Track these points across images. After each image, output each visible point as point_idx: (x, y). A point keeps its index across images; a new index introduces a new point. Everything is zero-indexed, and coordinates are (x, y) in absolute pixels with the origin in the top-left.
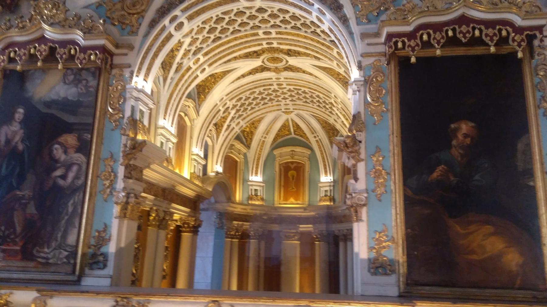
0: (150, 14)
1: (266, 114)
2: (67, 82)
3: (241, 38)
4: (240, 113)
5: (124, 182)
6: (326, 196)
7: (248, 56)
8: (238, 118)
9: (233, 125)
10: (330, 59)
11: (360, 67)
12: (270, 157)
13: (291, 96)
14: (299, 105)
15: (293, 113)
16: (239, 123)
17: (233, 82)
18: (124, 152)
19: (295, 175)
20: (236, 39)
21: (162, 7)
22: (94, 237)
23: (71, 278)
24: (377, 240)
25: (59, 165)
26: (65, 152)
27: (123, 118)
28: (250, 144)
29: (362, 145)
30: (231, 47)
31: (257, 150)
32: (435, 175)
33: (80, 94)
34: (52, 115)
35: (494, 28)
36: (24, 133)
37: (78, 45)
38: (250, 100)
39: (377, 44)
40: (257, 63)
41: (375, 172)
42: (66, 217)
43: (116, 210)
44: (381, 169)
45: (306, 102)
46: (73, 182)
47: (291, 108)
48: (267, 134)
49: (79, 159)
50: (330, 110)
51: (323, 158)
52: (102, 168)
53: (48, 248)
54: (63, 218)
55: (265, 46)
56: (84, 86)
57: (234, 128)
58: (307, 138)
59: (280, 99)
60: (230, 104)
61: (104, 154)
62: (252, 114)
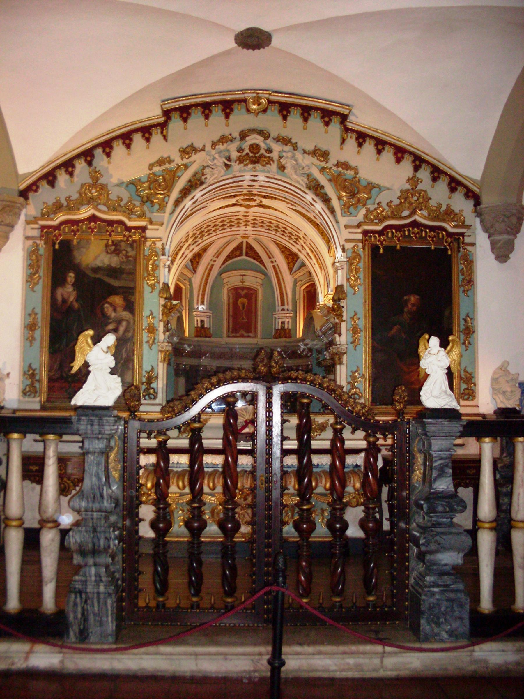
0: (175, 194)
2: (109, 251)
5: (164, 334)
9: (187, 252)
10: (307, 210)
11: (344, 250)
13: (254, 223)
15: (250, 238)
16: (193, 249)
19: (246, 304)
25: (110, 321)
26: (115, 310)
27: (159, 283)
28: (196, 268)
29: (344, 310)
33: (122, 263)
36: (77, 294)
38: (210, 228)
45: (269, 229)
48: (217, 257)
50: (295, 240)
56: (124, 255)
58: (262, 262)
59: (240, 225)
62: (207, 239)
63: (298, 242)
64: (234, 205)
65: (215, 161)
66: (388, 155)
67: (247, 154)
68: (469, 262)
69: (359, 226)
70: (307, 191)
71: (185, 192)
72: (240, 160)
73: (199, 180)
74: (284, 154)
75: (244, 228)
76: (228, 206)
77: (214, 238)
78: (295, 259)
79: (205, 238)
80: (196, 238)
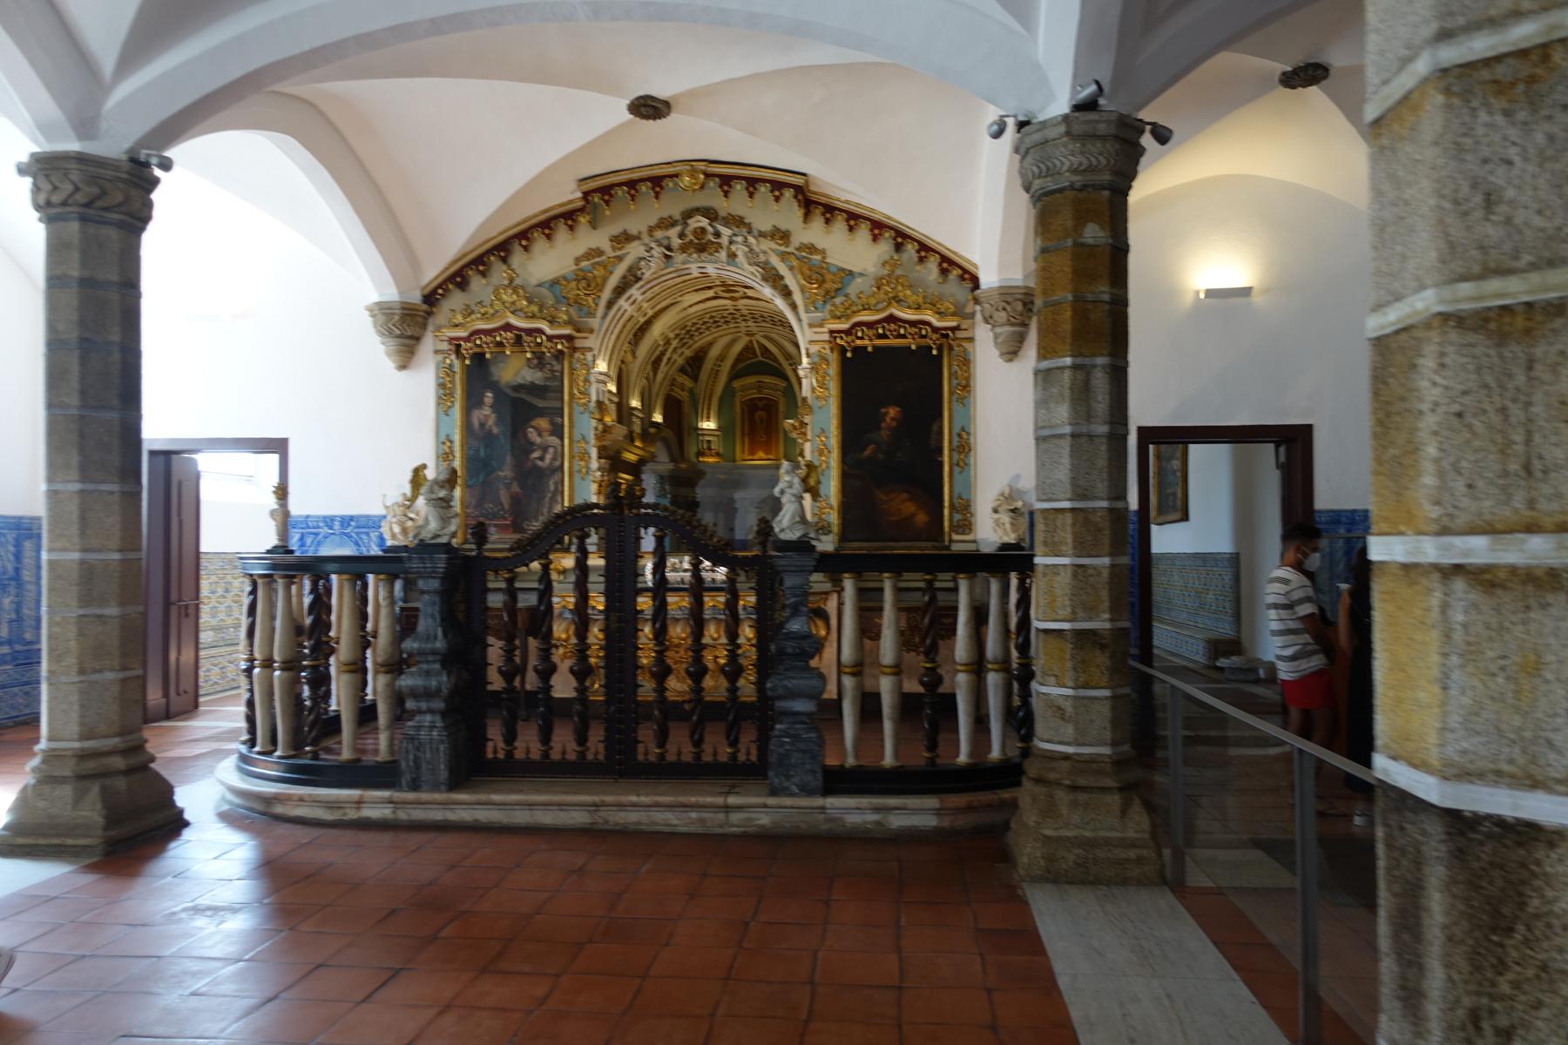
0: (606, 294)
7: (696, 290)
9: (675, 356)
12: (729, 392)
16: (682, 353)
18: (596, 435)
21: (618, 287)
26: (540, 435)
29: (809, 427)
32: (867, 452)
33: (547, 379)
34: (521, 399)
35: (915, 327)
40: (710, 293)
42: (549, 495)
48: (722, 361)
52: (576, 450)
60: (672, 335)
61: (577, 437)
65: (654, 252)
66: (864, 232)
68: (966, 362)
69: (821, 326)
71: (620, 291)
73: (635, 276)
74: (734, 238)
76: (708, 299)
77: (715, 335)
79: (696, 338)
80: (682, 339)
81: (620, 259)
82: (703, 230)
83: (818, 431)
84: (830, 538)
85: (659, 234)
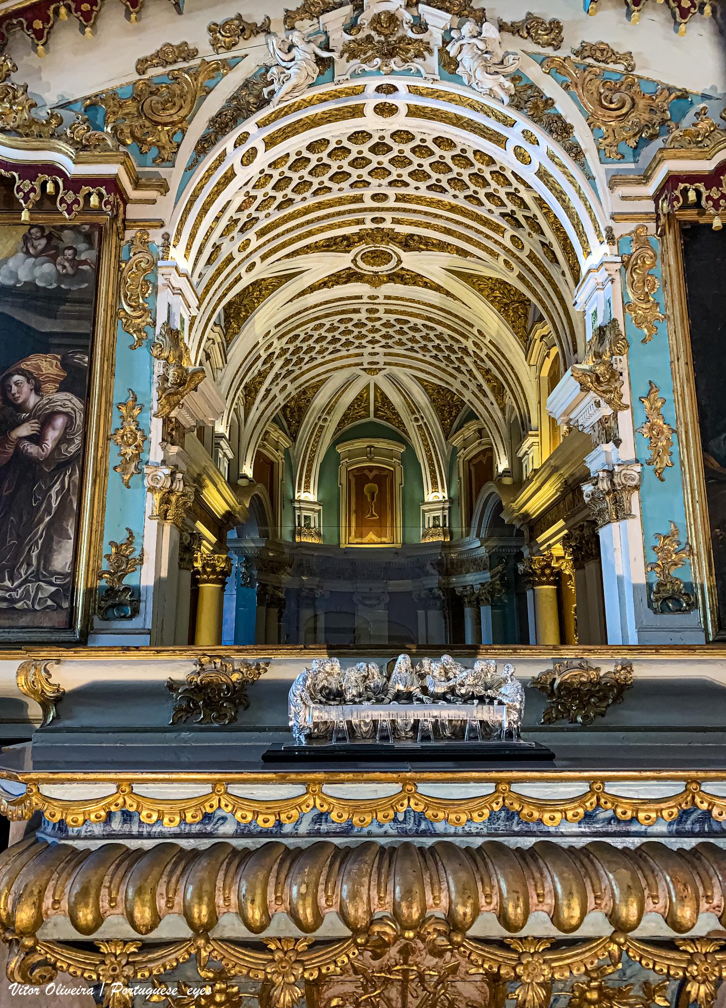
0: (198, 128)
1: (332, 373)
2: (31, 251)
3: (330, 205)
4: (290, 367)
5: (164, 449)
6: (435, 526)
7: (330, 245)
8: (284, 377)
12: (332, 459)
14: (398, 355)
15: (383, 372)
17: (291, 301)
20: (320, 206)
22: (108, 557)
23: (65, 636)
24: (662, 549)
26: (37, 390)
27: (154, 324)
28: (296, 432)
30: (308, 222)
31: (308, 443)
33: (61, 277)
37: (62, 174)
39: (639, 198)
41: (651, 429)
42: (47, 519)
43: (152, 502)
44: (661, 423)
46: (57, 448)
47: (381, 359)
48: (328, 413)
49: (67, 402)
51: (430, 459)
53: (12, 580)
54: (41, 520)
55: (369, 225)
56: (67, 260)
57: (275, 397)
61: (119, 394)
63: (463, 368)
64: (350, 276)
65: (294, 51)
67: (369, 38)
70: (512, 114)
72: (351, 53)
73: (259, 96)
75: (369, 349)
78: (453, 414)
81: (229, 65)
82: (392, 19)
83: (644, 389)
84: (696, 617)
85: (306, 25)
